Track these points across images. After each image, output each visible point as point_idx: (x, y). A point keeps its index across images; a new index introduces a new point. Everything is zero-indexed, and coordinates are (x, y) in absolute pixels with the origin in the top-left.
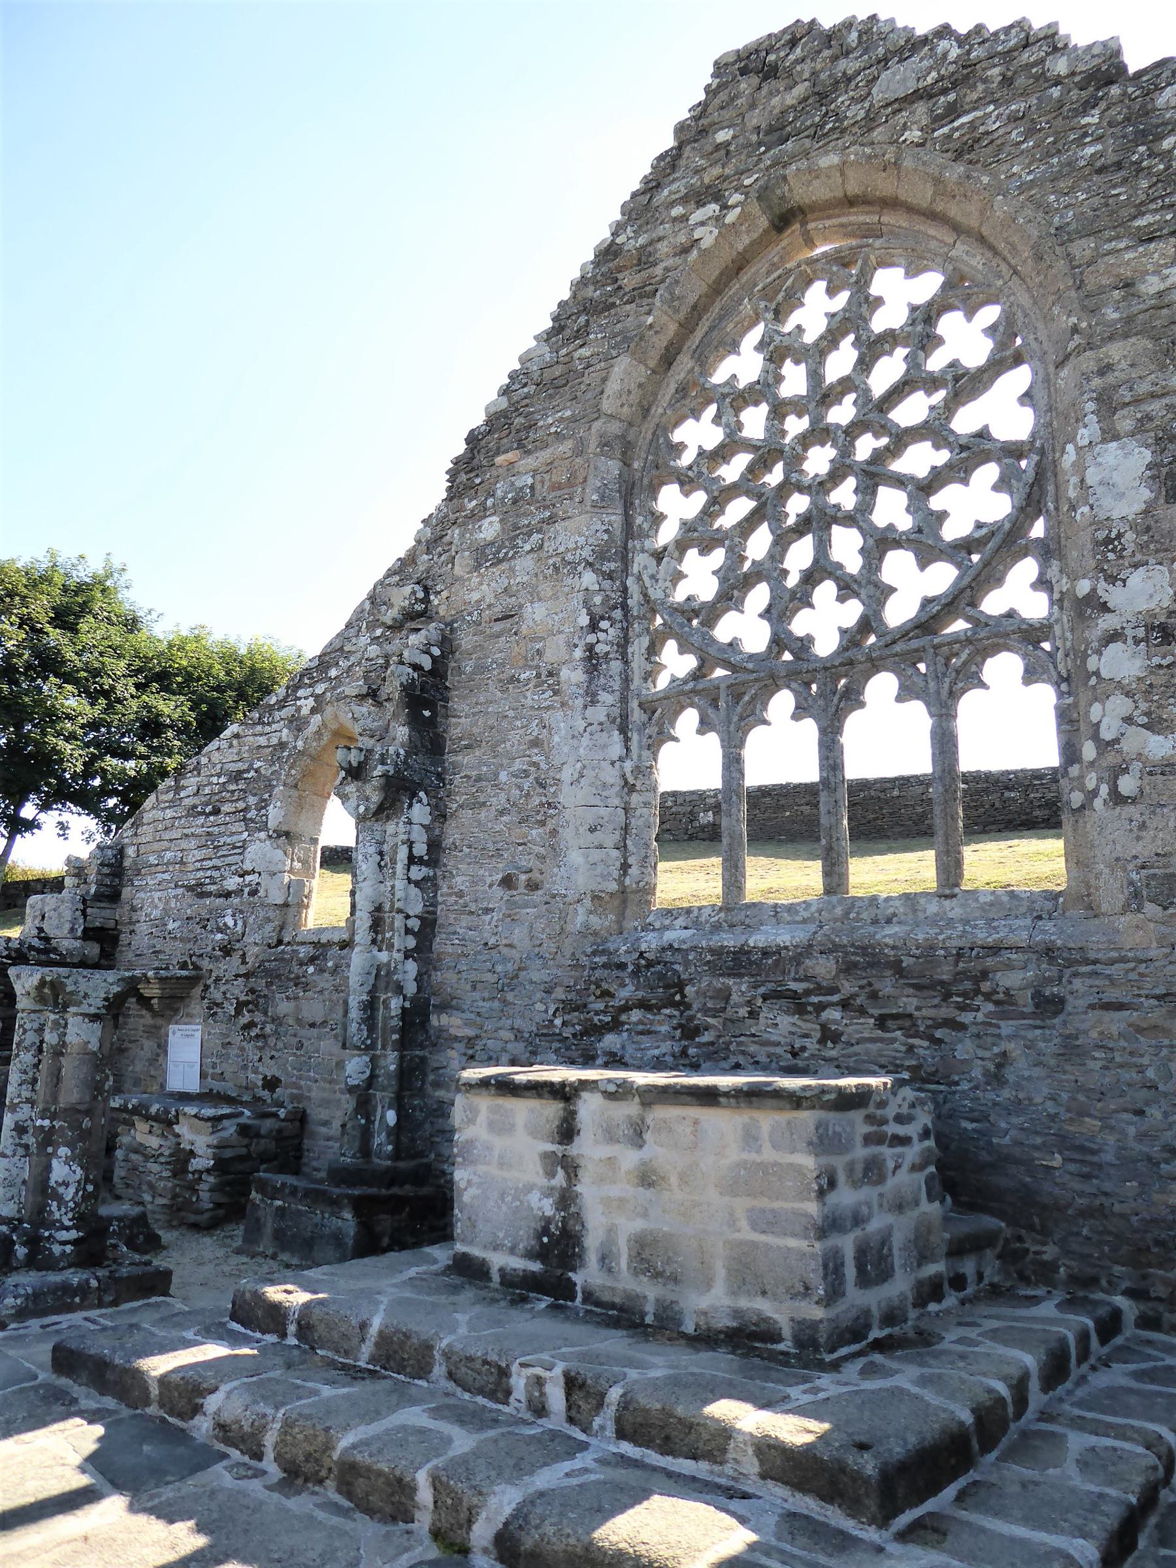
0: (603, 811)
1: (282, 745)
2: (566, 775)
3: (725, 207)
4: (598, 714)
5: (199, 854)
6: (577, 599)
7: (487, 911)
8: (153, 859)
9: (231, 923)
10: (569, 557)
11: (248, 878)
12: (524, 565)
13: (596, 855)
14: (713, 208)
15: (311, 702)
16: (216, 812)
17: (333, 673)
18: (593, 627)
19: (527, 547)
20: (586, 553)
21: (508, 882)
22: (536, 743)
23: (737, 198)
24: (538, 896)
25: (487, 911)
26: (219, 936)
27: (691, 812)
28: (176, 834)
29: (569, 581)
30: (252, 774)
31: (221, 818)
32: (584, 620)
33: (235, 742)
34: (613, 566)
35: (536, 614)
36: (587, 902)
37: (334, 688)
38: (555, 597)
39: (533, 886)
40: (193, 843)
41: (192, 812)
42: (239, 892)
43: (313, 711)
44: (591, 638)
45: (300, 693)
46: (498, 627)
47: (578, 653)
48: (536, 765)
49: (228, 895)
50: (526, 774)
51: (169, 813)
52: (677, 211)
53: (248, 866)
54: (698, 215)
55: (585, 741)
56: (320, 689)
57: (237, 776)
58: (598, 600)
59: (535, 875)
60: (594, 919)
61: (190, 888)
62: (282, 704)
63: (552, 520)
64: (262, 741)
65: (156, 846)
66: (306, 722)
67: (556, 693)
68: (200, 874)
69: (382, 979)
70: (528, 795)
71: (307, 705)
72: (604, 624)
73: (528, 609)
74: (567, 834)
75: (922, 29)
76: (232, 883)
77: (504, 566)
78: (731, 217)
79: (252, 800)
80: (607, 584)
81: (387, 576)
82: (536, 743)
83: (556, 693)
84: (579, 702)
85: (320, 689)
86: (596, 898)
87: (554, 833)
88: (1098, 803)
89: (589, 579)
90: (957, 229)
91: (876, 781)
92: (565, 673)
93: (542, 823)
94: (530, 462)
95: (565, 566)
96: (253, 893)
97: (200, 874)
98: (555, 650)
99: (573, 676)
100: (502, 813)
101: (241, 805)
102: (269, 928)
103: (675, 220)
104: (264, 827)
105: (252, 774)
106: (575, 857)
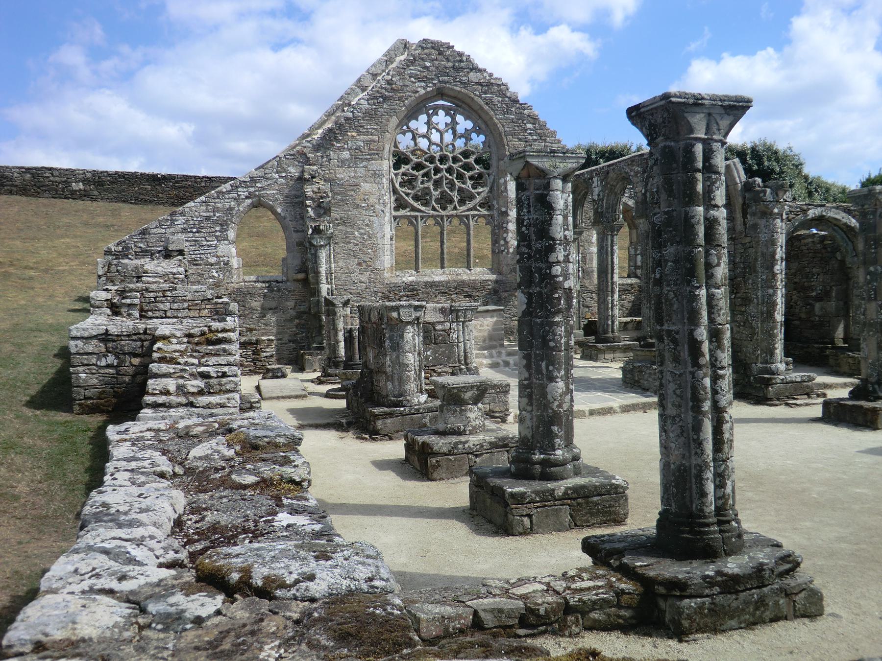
1: (231, 209)
2: (379, 235)
5: (192, 248)
9: (216, 275)
12: (361, 171)
14: (423, 84)
22: (367, 225)
26: (211, 280)
27: (66, 182)
30: (215, 218)
42: (218, 263)
43: (247, 197)
49: (212, 265)
56: (252, 190)
57: (208, 218)
64: (219, 205)
68: (193, 256)
75: (481, 66)
76: (213, 260)
78: (429, 89)
79: (218, 229)
83: (374, 212)
85: (252, 190)
88: (504, 253)
90: (480, 117)
91: (191, 177)
93: (372, 249)
96: (226, 264)
97: (193, 256)
103: (413, 82)
104: (226, 239)
105: (215, 218)
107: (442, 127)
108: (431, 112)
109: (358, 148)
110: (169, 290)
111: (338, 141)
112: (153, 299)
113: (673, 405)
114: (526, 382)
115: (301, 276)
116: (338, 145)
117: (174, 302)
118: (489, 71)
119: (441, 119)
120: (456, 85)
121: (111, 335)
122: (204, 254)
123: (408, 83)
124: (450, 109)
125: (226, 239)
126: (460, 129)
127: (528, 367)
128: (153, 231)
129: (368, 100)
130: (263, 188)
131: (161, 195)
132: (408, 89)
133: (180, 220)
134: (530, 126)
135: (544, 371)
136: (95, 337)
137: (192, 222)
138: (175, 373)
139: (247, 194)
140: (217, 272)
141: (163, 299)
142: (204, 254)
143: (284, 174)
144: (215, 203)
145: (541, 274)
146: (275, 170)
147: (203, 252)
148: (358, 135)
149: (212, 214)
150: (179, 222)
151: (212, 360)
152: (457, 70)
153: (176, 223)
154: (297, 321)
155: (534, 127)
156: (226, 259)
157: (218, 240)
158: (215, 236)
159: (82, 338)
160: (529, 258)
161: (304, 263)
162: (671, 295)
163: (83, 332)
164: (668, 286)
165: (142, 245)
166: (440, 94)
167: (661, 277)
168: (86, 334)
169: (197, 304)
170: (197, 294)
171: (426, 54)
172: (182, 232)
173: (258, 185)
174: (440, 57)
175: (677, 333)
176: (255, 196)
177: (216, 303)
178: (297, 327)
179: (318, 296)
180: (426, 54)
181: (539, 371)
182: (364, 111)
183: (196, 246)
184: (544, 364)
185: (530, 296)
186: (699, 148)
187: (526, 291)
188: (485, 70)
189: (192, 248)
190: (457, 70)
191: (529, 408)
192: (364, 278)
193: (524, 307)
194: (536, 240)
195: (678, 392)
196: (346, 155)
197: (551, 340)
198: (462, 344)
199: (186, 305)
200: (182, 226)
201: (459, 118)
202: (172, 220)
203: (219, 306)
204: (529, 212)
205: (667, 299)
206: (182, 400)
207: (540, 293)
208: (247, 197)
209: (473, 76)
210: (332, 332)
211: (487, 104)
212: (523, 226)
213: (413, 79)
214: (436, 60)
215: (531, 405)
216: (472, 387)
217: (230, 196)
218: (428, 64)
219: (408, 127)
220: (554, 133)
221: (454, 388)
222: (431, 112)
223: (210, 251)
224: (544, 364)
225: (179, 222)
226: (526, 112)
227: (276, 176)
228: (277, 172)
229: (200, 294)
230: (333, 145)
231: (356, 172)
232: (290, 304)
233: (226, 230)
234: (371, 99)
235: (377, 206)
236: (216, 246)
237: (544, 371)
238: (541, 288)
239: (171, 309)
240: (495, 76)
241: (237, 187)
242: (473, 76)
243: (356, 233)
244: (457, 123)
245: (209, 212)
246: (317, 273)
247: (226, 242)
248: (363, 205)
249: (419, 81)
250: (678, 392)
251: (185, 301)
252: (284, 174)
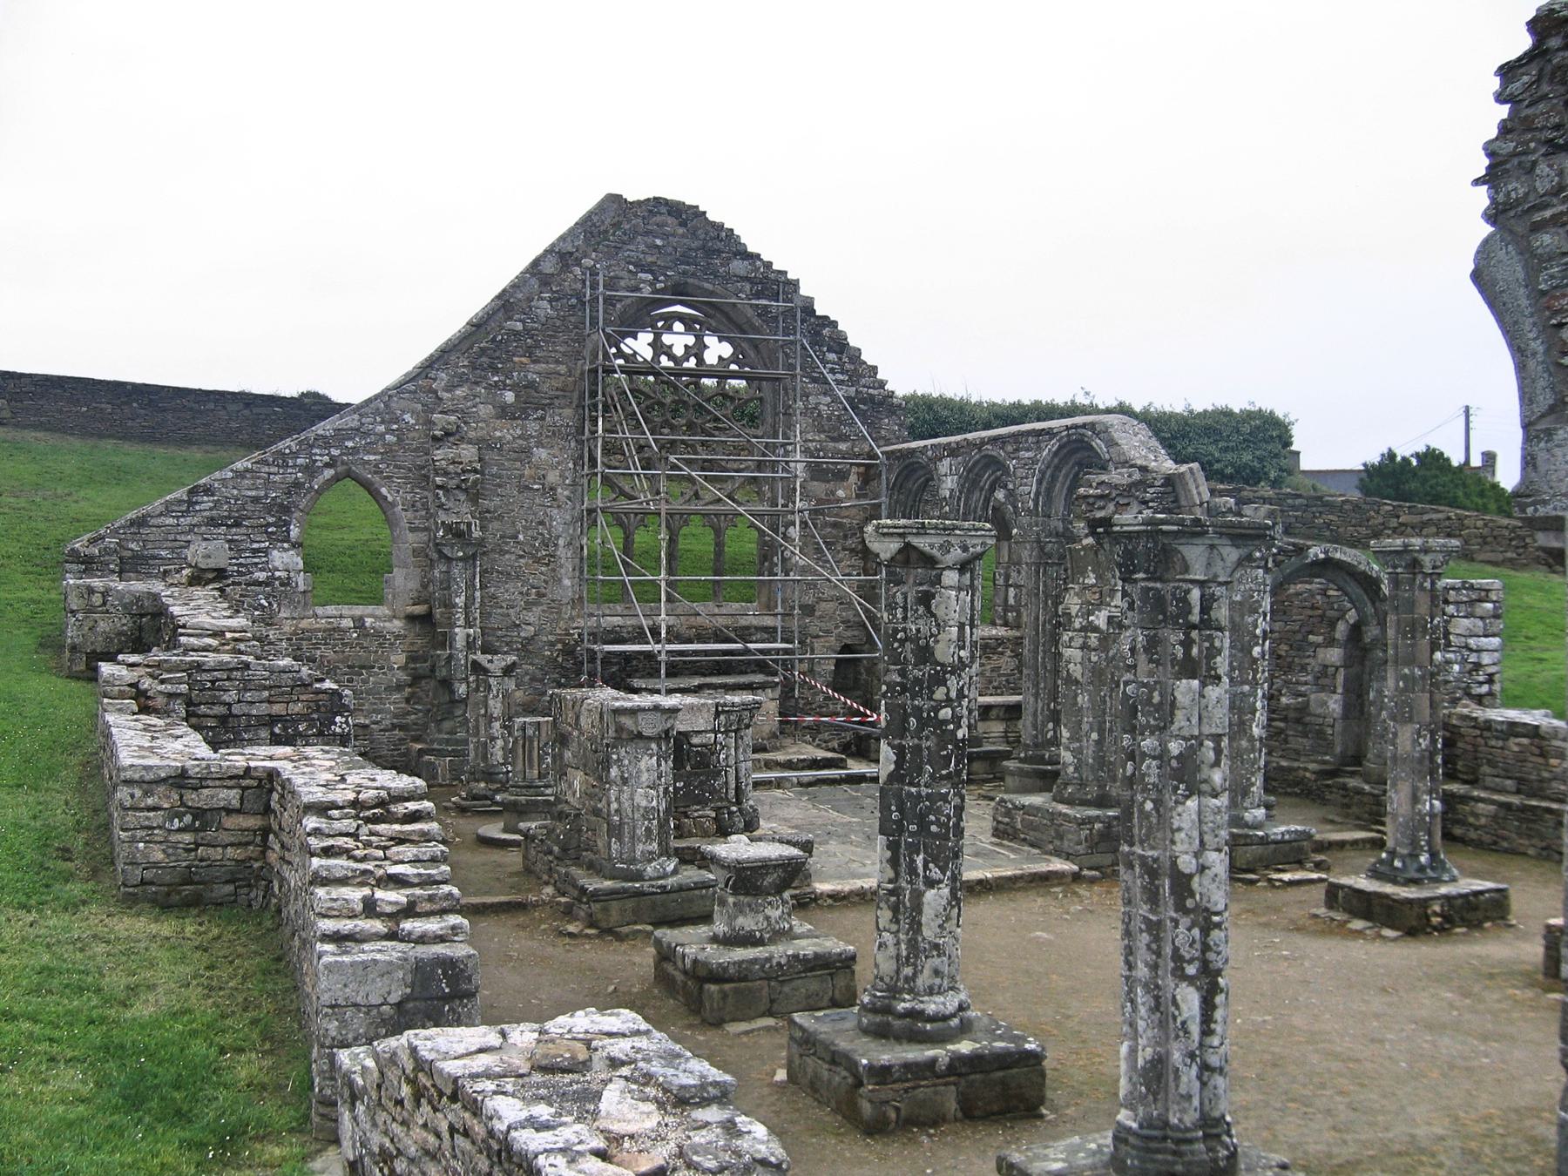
1: (297, 484)
3: (656, 279)
12: (533, 427)
14: (650, 277)
16: (237, 524)
22: (541, 523)
23: (662, 278)
42: (266, 583)
43: (327, 465)
49: (260, 584)
52: (631, 267)
54: (642, 275)
56: (335, 452)
57: (256, 500)
66: (320, 470)
76: (262, 576)
79: (271, 520)
82: (541, 523)
83: (554, 500)
85: (335, 452)
87: (554, 570)
93: (547, 565)
94: (539, 367)
103: (630, 271)
104: (287, 539)
107: (679, 351)
108: (660, 324)
109: (531, 385)
110: (238, 669)
111: (496, 371)
112: (209, 685)
113: (1147, 965)
114: (890, 886)
115: (419, 609)
116: (496, 379)
117: (246, 690)
118: (765, 257)
119: (678, 341)
120: (707, 280)
121: (190, 778)
123: (624, 274)
124: (695, 320)
125: (287, 539)
126: (711, 358)
127: (894, 862)
128: (153, 521)
129: (550, 301)
130: (355, 451)
131: (130, 423)
132: (622, 283)
133: (206, 502)
134: (832, 356)
135: (921, 870)
136: (164, 780)
137: (225, 507)
138: (353, 877)
139: (326, 459)
141: (227, 683)
143: (395, 427)
144: (269, 474)
145: (919, 719)
146: (378, 419)
148: (534, 362)
149: (262, 493)
150: (203, 506)
151: (408, 851)
152: (710, 253)
153: (197, 508)
154: (408, 690)
155: (840, 359)
156: (283, 574)
158: (266, 532)
159: (140, 782)
160: (904, 689)
161: (425, 586)
162: (1149, 806)
163: (144, 773)
164: (1143, 791)
165: (133, 546)
166: (679, 291)
167: (1134, 774)
168: (150, 776)
169: (283, 694)
170: (285, 676)
171: (658, 225)
172: (207, 525)
173: (350, 444)
174: (681, 231)
175: (1155, 860)
176: (343, 463)
177: (319, 692)
178: (408, 701)
179: (451, 648)
180: (658, 225)
181: (913, 871)
182: (544, 320)
184: (919, 860)
185: (900, 752)
186: (1195, 594)
187: (897, 742)
188: (758, 256)
190: (710, 253)
191: (894, 927)
193: (892, 767)
194: (915, 665)
195: (1154, 946)
196: (509, 397)
197: (932, 823)
198: (732, 771)
199: (266, 693)
200: (207, 514)
201: (711, 340)
202: (191, 503)
203: (321, 696)
204: (905, 618)
205: (1141, 811)
206: (378, 926)
207: (918, 748)
208: (327, 465)
209: (738, 266)
210: (482, 721)
211: (759, 315)
212: (896, 640)
213: (631, 267)
214: (673, 235)
215: (897, 922)
216: (775, 867)
217: (299, 461)
218: (658, 242)
219: (619, 349)
220: (874, 369)
221: (748, 868)
222: (660, 324)
223: (257, 560)
224: (919, 860)
225: (203, 506)
226: (826, 331)
227: (382, 428)
228: (382, 422)
229: (290, 675)
230: (485, 378)
231: (523, 427)
232: (399, 659)
233: (287, 524)
234: (557, 300)
235: (559, 490)
236: (266, 552)
237: (921, 870)
238: (920, 739)
239: (239, 701)
240: (775, 267)
241: (312, 446)
242: (738, 266)
243: (521, 537)
244: (706, 347)
245: (257, 489)
246: (449, 605)
247: (286, 545)
248: (536, 487)
249: (643, 271)
250: (1154, 946)
251: (265, 688)
252: (395, 427)
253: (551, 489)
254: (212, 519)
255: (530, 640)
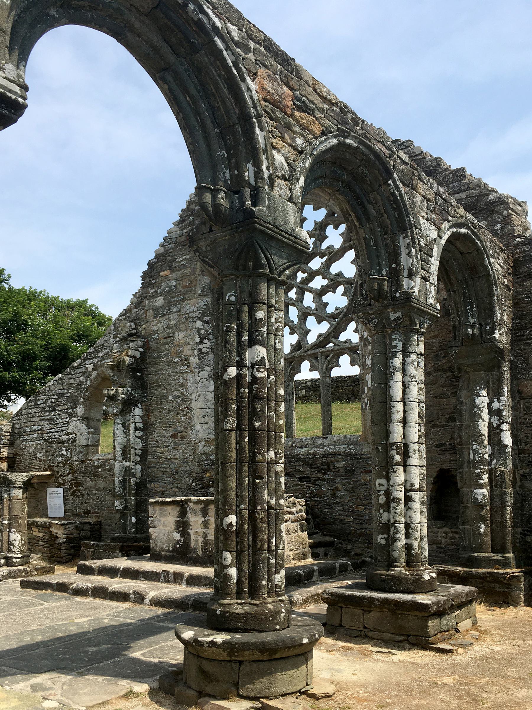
0: (208, 410)
1: (81, 383)
2: (193, 397)
4: (205, 375)
5: (48, 427)
6: (195, 331)
7: (167, 447)
8: (28, 429)
9: (65, 453)
10: (191, 315)
11: (71, 436)
13: (206, 426)
15: (92, 366)
16: (54, 410)
17: (100, 354)
18: (201, 342)
19: (175, 310)
20: (197, 314)
21: (174, 436)
22: (182, 385)
24: (184, 441)
25: (167, 447)
26: (60, 459)
28: (37, 419)
29: (191, 324)
30: (69, 394)
31: (57, 412)
32: (198, 340)
33: (60, 382)
34: (208, 318)
35: (180, 336)
36: (203, 442)
37: (101, 361)
38: (186, 330)
39: (183, 438)
40: (45, 423)
41: (43, 410)
42: (68, 441)
44: (200, 347)
45: (87, 362)
46: (165, 341)
47: (196, 352)
48: (182, 394)
49: (63, 442)
50: (178, 397)
51: (34, 410)
53: (70, 431)
55: (200, 385)
57: (62, 395)
58: (202, 332)
59: (184, 434)
60: (205, 448)
61: (46, 440)
62: (79, 367)
63: (183, 300)
64: (72, 381)
65: (29, 424)
67: (188, 367)
68: (49, 435)
69: (127, 473)
70: (179, 405)
71: (90, 367)
72: (205, 341)
73: (176, 334)
74: (195, 418)
76: (65, 438)
77: (167, 317)
79: (70, 405)
80: (206, 325)
81: (120, 316)
82: (182, 385)
84: (197, 370)
86: (206, 441)
87: (190, 418)
89: (199, 324)
92: (191, 359)
93: (185, 415)
95: (189, 319)
96: (74, 441)
97: (49, 435)
98: (187, 351)
99: (194, 360)
100: (170, 411)
101: (65, 407)
102: (81, 455)
105: (69, 394)
106: (198, 427)
122: (57, 432)
140: (66, 451)
142: (57, 432)
147: (57, 430)
153: (39, 403)
157: (71, 417)
158: (67, 413)
183: (52, 424)
189: (48, 427)
192: (178, 454)
253: (186, 360)
254: (44, 408)
255: (176, 470)
